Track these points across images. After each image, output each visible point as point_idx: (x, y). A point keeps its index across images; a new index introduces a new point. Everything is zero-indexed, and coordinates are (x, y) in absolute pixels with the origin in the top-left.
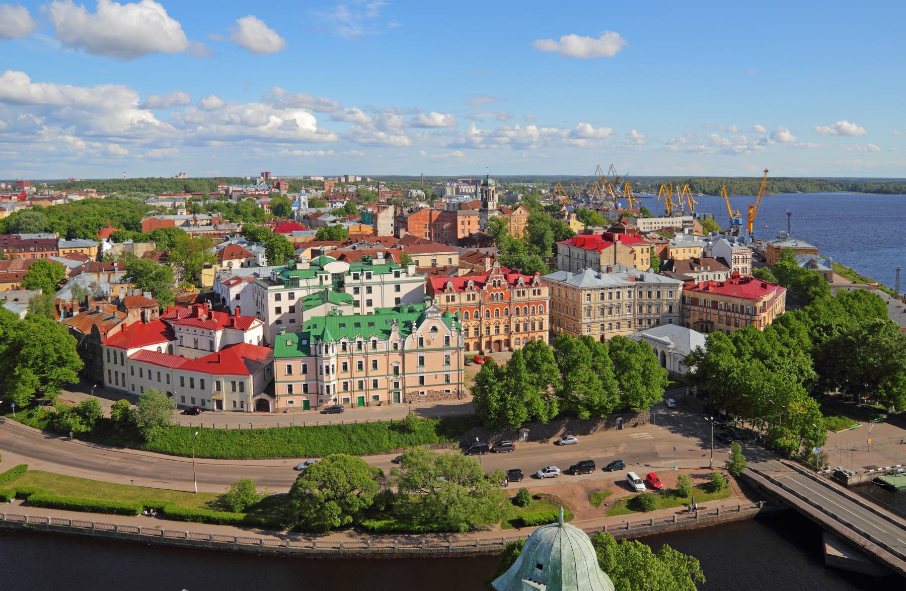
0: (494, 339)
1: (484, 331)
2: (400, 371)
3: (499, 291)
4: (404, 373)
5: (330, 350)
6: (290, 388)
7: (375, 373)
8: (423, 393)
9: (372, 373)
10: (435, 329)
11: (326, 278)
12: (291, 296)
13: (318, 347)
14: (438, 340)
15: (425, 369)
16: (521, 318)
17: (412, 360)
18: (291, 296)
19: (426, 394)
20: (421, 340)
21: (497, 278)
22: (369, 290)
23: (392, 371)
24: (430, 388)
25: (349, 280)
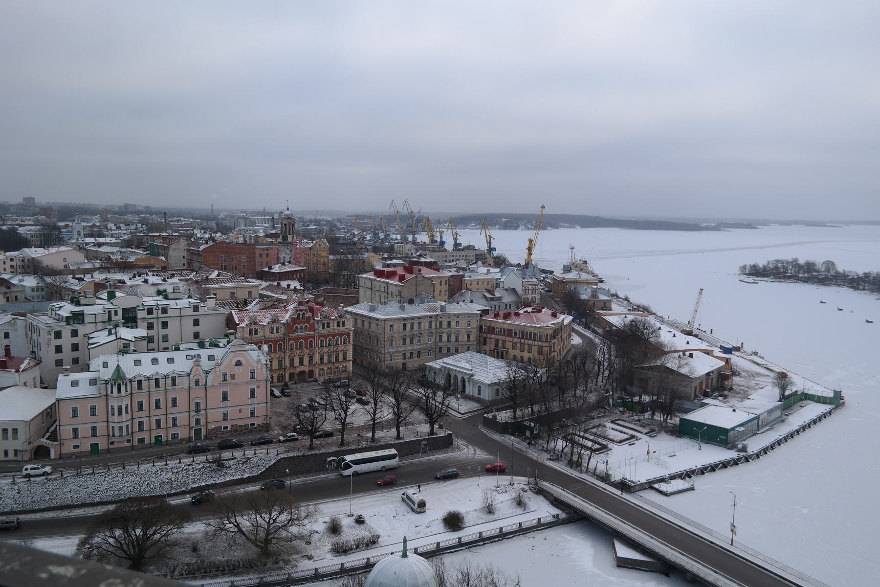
0: (298, 370)
1: (288, 363)
2: (202, 406)
3: (304, 323)
4: (206, 409)
5: (123, 389)
6: (75, 431)
7: (174, 410)
8: (226, 428)
9: (171, 410)
10: (239, 363)
11: (116, 314)
12: (74, 333)
13: (109, 386)
14: (242, 373)
15: (228, 404)
16: (326, 350)
17: (215, 398)
18: (74, 333)
19: (229, 429)
20: (225, 375)
21: (301, 310)
22: (165, 325)
23: (193, 408)
24: (234, 423)
25: (141, 314)
